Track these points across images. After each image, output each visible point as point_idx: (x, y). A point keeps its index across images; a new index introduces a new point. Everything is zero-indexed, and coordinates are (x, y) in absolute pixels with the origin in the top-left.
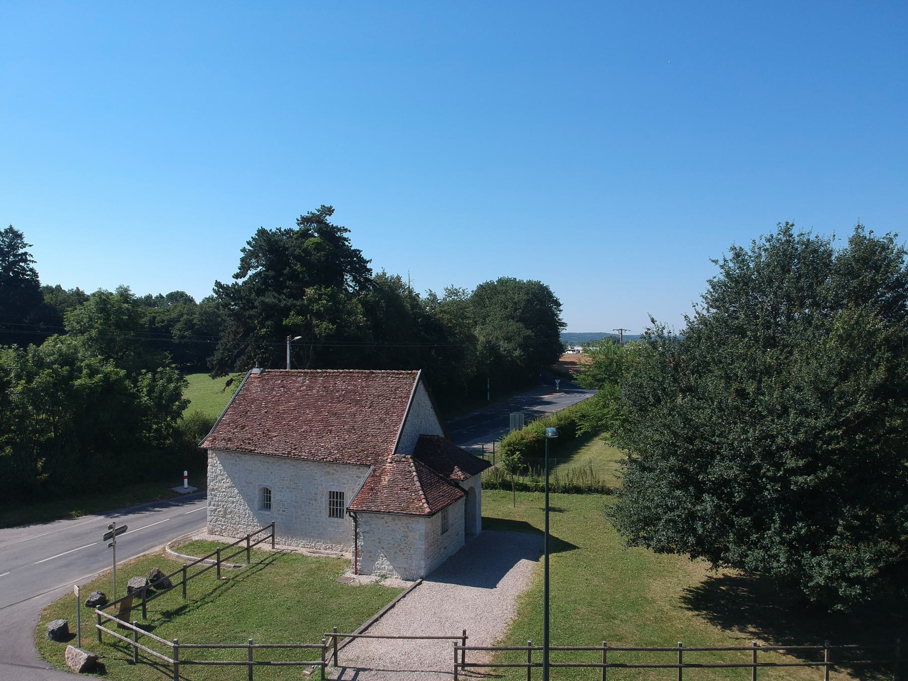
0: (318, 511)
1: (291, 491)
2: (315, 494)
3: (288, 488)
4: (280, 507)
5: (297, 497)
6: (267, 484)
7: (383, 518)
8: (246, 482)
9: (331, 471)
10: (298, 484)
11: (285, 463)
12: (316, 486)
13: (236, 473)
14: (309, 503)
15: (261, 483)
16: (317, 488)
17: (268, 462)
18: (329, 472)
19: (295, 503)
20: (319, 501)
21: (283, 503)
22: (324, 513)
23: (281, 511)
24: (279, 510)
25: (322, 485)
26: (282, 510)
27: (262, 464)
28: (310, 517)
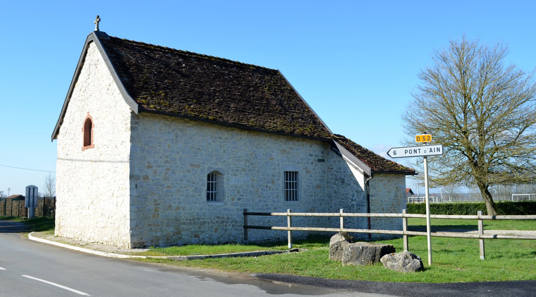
0: (275, 195)
1: (247, 174)
2: (273, 175)
3: (244, 170)
4: (235, 195)
5: (254, 180)
6: (218, 166)
7: (382, 181)
8: (192, 165)
9: (287, 150)
10: (254, 165)
11: (241, 139)
12: (273, 167)
13: (178, 153)
14: (267, 187)
15: (212, 166)
17: (220, 138)
19: (252, 187)
20: (276, 184)
21: (238, 189)
22: (281, 197)
23: (236, 201)
24: (233, 199)
25: (279, 165)
26: (236, 198)
27: (214, 141)
28: (268, 203)
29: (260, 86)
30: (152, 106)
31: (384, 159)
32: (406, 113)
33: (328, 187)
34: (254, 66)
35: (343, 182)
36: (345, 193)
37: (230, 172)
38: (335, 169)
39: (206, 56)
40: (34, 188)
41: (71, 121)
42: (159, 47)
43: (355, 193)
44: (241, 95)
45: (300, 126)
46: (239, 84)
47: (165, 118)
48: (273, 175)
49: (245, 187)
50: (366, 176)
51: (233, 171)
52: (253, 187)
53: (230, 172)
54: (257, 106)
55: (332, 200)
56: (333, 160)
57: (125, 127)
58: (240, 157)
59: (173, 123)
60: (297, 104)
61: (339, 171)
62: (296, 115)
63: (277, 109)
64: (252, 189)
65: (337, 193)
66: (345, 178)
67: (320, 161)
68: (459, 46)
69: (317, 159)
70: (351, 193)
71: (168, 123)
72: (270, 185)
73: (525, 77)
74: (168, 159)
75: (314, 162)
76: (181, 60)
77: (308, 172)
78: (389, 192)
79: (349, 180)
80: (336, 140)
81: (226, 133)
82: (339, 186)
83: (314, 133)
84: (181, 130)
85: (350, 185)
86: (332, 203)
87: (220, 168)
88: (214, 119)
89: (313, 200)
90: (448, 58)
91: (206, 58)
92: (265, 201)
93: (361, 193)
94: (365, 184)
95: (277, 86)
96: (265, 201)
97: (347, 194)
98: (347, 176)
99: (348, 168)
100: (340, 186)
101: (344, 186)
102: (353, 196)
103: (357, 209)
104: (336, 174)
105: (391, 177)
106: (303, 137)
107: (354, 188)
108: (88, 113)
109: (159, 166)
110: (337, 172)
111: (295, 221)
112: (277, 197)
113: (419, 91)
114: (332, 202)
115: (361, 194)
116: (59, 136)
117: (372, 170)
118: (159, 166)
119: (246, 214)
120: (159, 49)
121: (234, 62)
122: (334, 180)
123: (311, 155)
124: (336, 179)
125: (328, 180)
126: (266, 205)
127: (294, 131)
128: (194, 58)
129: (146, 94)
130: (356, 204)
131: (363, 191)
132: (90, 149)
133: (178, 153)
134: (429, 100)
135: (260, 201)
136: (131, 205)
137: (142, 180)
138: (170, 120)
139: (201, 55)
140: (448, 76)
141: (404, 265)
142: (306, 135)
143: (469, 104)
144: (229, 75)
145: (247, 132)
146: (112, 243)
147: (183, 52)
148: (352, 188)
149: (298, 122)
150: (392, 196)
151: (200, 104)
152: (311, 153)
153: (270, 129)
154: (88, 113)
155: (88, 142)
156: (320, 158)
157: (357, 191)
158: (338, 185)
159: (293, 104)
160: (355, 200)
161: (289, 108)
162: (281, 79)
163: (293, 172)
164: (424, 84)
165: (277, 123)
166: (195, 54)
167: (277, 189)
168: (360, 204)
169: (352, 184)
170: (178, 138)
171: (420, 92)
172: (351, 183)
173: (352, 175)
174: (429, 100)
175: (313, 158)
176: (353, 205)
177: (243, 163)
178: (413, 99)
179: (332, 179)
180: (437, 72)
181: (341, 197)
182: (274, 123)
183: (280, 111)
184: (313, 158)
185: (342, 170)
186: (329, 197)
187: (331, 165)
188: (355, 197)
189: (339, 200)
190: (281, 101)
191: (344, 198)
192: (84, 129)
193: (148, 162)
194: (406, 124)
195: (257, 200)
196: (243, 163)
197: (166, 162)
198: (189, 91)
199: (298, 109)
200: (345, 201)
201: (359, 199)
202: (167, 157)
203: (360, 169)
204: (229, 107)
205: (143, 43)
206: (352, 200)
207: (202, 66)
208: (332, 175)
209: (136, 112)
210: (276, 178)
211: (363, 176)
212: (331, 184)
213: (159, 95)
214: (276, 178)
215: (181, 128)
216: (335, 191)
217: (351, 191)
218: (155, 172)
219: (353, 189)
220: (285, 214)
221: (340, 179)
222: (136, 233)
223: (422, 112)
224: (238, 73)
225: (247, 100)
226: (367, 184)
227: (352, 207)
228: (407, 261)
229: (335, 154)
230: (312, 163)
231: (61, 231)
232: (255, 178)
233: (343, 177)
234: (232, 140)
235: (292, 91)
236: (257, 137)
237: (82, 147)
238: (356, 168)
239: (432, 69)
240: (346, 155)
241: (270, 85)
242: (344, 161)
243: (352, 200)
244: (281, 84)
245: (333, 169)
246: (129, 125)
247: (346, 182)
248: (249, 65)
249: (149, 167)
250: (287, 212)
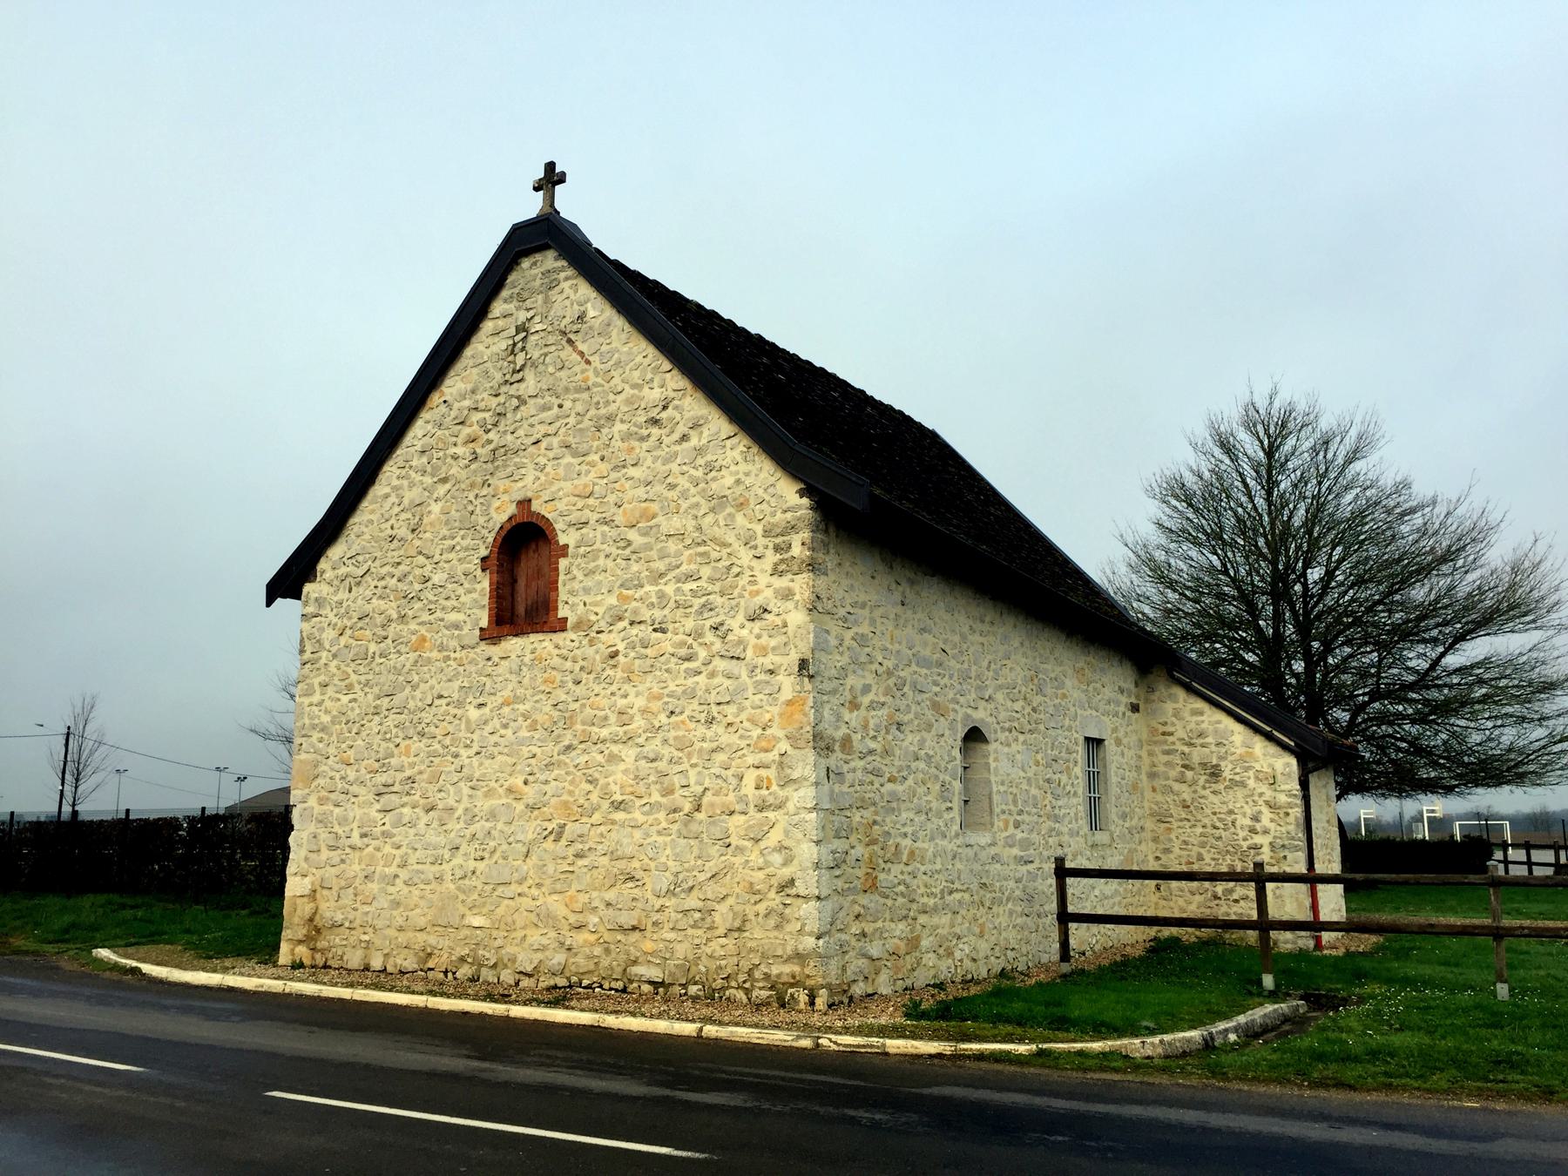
33: (1154, 790)
35: (1215, 773)
36: (1225, 809)
41: (403, 532)
43: (1265, 810)
56: (1169, 707)
57: (771, 558)
65: (1192, 808)
66: (1223, 764)
67: (1135, 708)
70: (1249, 811)
73: (1441, 510)
79: (1238, 770)
82: (1199, 789)
85: (1243, 784)
86: (1170, 840)
87: (983, 720)
93: (1290, 811)
98: (1230, 758)
100: (1204, 788)
101: (1221, 787)
102: (1256, 819)
103: (1271, 858)
107: (1261, 795)
110: (1191, 745)
114: (1173, 836)
115: (1287, 814)
119: (1062, 872)
122: (1179, 769)
124: (1184, 766)
125: (1155, 769)
130: (1271, 843)
148: (1252, 795)
158: (1195, 782)
160: (1266, 832)
168: (1286, 843)
169: (1251, 783)
172: (1249, 778)
176: (1257, 847)
181: (1206, 821)
185: (1210, 740)
186: (1160, 821)
187: (1165, 724)
188: (1266, 820)
189: (1199, 830)
191: (1218, 824)
201: (1279, 828)
208: (1167, 753)
212: (1167, 779)
216: (1184, 801)
217: (1247, 803)
219: (1256, 798)
221: (1203, 765)
227: (1252, 851)
231: (321, 944)
233: (1214, 762)
237: (484, 623)
243: (1253, 831)
245: (1171, 734)
247: (1227, 774)
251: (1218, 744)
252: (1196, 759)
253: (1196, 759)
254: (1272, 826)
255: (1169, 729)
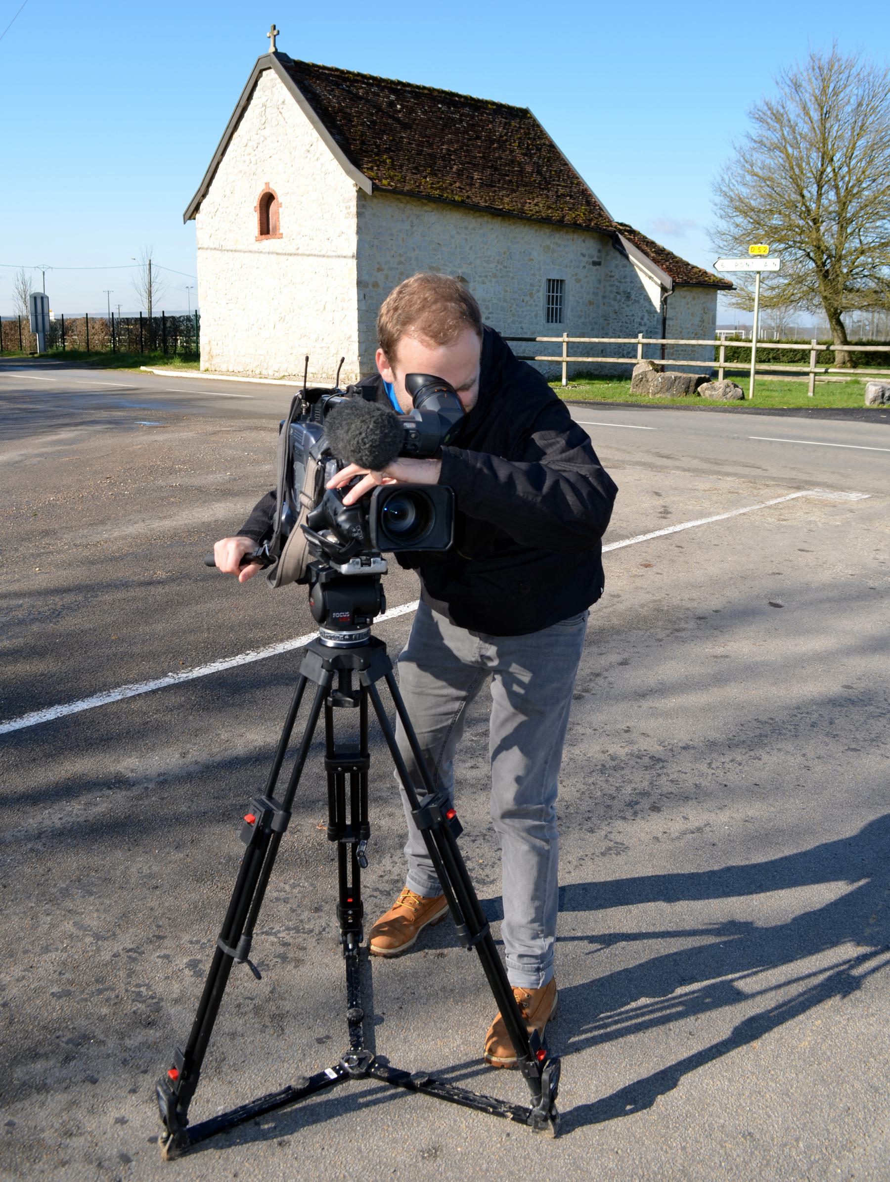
0: (533, 314)
2: (532, 285)
3: (495, 276)
9: (552, 246)
12: (532, 272)
16: (534, 275)
17: (466, 228)
18: (548, 247)
20: (535, 297)
25: (540, 269)
28: (524, 326)
29: (506, 140)
30: (385, 182)
31: (688, 264)
32: (719, 180)
34: (493, 103)
35: (628, 297)
37: (477, 279)
38: (617, 277)
39: (424, 88)
40: (42, 298)
42: (359, 74)
43: (646, 314)
44: (483, 157)
45: (570, 209)
46: (478, 138)
47: (398, 199)
48: (532, 285)
49: (495, 301)
50: (664, 289)
51: (480, 276)
52: (505, 301)
53: (477, 279)
54: (508, 176)
55: (608, 324)
58: (490, 257)
59: (409, 206)
60: (561, 170)
61: (623, 280)
62: (561, 191)
63: (535, 181)
64: (505, 304)
67: (595, 263)
68: (824, 62)
69: (591, 260)
70: (640, 315)
71: (402, 206)
72: (527, 298)
74: (402, 259)
75: (587, 266)
76: (393, 97)
77: (578, 281)
78: (693, 315)
80: (620, 231)
81: (474, 220)
83: (590, 220)
84: (418, 217)
85: (638, 302)
88: (463, 201)
89: (583, 323)
90: (803, 84)
91: (426, 92)
92: (520, 323)
94: (661, 302)
95: (529, 138)
96: (520, 323)
97: (633, 315)
99: (637, 276)
101: (630, 303)
102: (642, 319)
104: (619, 284)
105: (698, 292)
106: (575, 227)
108: (267, 184)
109: (391, 269)
110: (620, 282)
111: (573, 349)
112: (536, 316)
113: (747, 140)
116: (198, 216)
117: (674, 281)
118: (391, 269)
120: (359, 78)
121: (466, 98)
123: (584, 255)
124: (617, 293)
126: (522, 328)
127: (564, 217)
128: (411, 92)
129: (370, 162)
131: (656, 312)
132: (272, 240)
133: (414, 250)
134: (762, 159)
135: (514, 322)
136: (359, 322)
137: (371, 287)
138: (404, 201)
139: (418, 87)
140: (798, 116)
141: (725, 394)
142: (580, 225)
143: (829, 169)
144: (461, 121)
145: (500, 218)
146: (324, 375)
147: (392, 82)
149: (565, 202)
150: (697, 320)
151: (436, 175)
152: (584, 251)
153: (533, 215)
154: (267, 184)
155: (265, 229)
156: (596, 259)
157: (649, 312)
158: (620, 301)
159: (555, 171)
160: (645, 325)
161: (551, 177)
162: (533, 125)
163: (558, 281)
164: (755, 129)
165: (535, 205)
166: (409, 85)
167: (536, 305)
169: (642, 301)
170: (415, 228)
171: (747, 144)
173: (642, 287)
174: (762, 159)
175: (586, 259)
177: (493, 265)
178: (734, 155)
179: (611, 292)
180: (781, 111)
181: (623, 320)
182: (536, 205)
183: (540, 184)
184: (586, 259)
188: (645, 320)
189: (620, 324)
190: (539, 166)
192: (258, 208)
193: (378, 263)
194: (719, 199)
195: (510, 321)
196: (493, 265)
197: (400, 263)
198: (418, 154)
199: (563, 180)
200: (630, 326)
202: (400, 255)
203: (655, 278)
204: (472, 178)
205: (337, 70)
206: (640, 324)
207: (423, 107)
208: (611, 286)
209: (368, 189)
210: (535, 288)
211: (659, 289)
213: (384, 162)
214: (535, 288)
215: (418, 213)
218: (387, 277)
220: (560, 339)
221: (624, 292)
222: (365, 360)
223: (748, 178)
224: (473, 117)
225: (492, 166)
226: (664, 302)
228: (728, 390)
229: (618, 255)
230: (584, 267)
232: (508, 289)
234: (481, 231)
235: (552, 147)
236: (513, 227)
238: (650, 278)
239: (773, 103)
240: (635, 258)
241: (520, 138)
242: (632, 265)
243: (640, 324)
244: (535, 135)
246: (354, 210)
247: (633, 297)
248: (487, 102)
249: (380, 270)
250: (562, 336)
251: (631, 282)
252: (621, 289)
253: (621, 289)
254: (648, 322)
255: (613, 274)
